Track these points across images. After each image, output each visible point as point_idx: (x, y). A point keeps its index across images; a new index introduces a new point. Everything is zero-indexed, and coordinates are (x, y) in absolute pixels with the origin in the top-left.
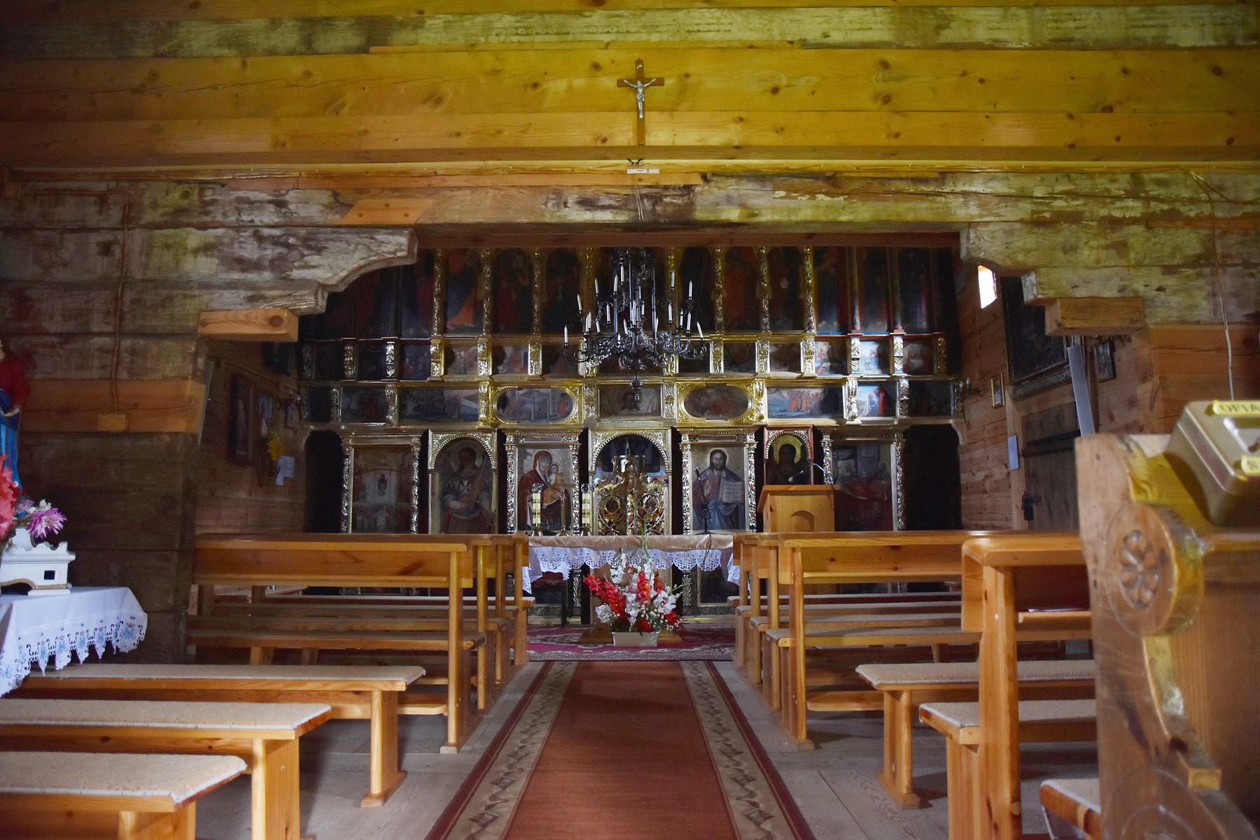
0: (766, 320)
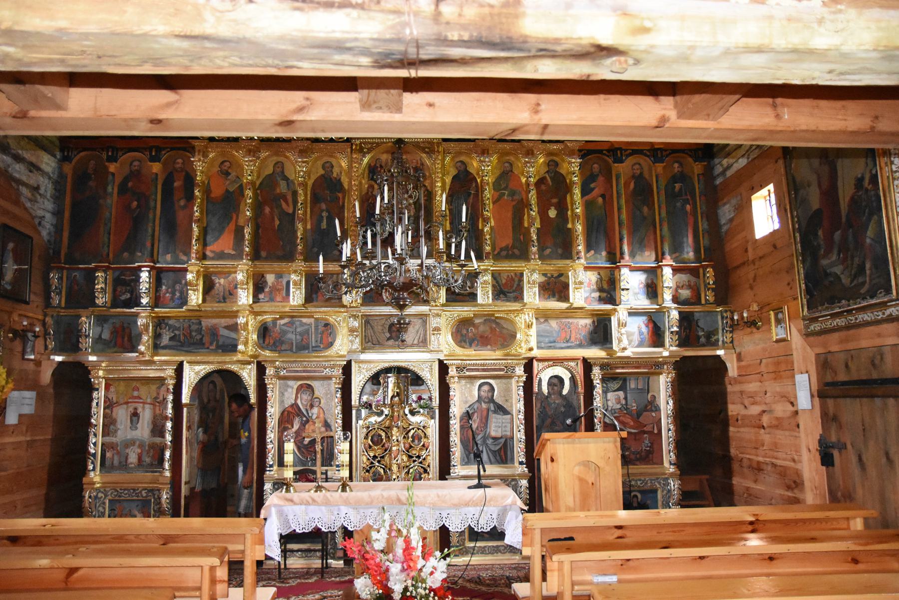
0: (534, 249)
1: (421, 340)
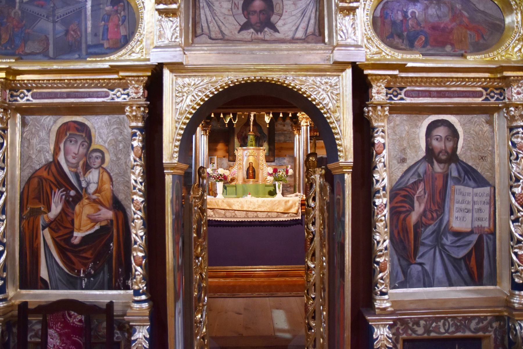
1: (310, 30)
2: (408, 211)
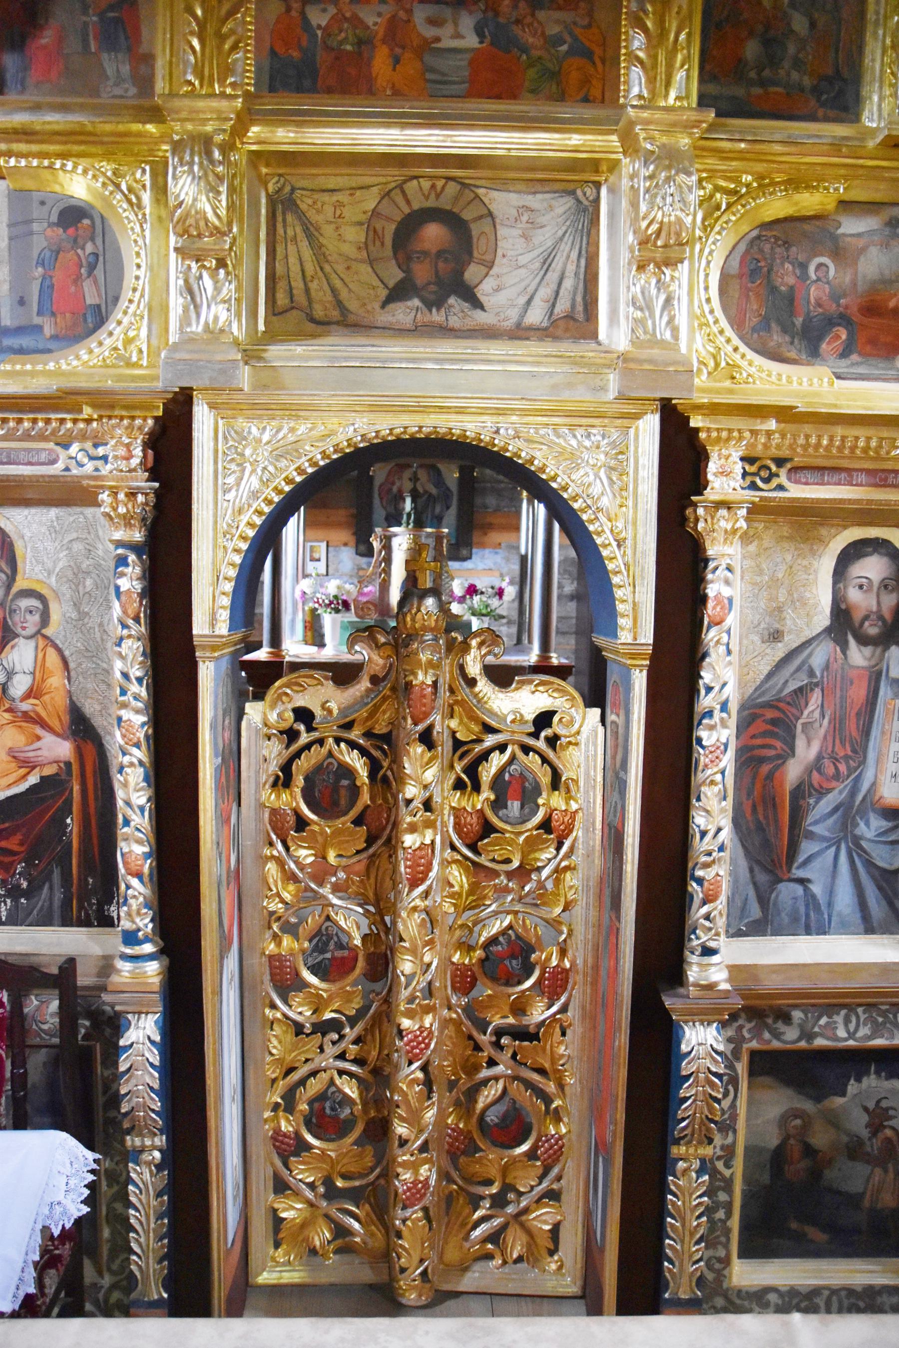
1: (562, 307)
2: (779, 757)
